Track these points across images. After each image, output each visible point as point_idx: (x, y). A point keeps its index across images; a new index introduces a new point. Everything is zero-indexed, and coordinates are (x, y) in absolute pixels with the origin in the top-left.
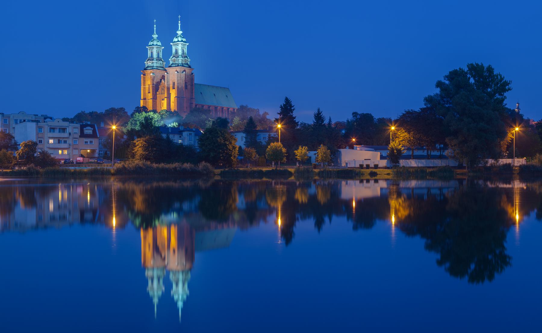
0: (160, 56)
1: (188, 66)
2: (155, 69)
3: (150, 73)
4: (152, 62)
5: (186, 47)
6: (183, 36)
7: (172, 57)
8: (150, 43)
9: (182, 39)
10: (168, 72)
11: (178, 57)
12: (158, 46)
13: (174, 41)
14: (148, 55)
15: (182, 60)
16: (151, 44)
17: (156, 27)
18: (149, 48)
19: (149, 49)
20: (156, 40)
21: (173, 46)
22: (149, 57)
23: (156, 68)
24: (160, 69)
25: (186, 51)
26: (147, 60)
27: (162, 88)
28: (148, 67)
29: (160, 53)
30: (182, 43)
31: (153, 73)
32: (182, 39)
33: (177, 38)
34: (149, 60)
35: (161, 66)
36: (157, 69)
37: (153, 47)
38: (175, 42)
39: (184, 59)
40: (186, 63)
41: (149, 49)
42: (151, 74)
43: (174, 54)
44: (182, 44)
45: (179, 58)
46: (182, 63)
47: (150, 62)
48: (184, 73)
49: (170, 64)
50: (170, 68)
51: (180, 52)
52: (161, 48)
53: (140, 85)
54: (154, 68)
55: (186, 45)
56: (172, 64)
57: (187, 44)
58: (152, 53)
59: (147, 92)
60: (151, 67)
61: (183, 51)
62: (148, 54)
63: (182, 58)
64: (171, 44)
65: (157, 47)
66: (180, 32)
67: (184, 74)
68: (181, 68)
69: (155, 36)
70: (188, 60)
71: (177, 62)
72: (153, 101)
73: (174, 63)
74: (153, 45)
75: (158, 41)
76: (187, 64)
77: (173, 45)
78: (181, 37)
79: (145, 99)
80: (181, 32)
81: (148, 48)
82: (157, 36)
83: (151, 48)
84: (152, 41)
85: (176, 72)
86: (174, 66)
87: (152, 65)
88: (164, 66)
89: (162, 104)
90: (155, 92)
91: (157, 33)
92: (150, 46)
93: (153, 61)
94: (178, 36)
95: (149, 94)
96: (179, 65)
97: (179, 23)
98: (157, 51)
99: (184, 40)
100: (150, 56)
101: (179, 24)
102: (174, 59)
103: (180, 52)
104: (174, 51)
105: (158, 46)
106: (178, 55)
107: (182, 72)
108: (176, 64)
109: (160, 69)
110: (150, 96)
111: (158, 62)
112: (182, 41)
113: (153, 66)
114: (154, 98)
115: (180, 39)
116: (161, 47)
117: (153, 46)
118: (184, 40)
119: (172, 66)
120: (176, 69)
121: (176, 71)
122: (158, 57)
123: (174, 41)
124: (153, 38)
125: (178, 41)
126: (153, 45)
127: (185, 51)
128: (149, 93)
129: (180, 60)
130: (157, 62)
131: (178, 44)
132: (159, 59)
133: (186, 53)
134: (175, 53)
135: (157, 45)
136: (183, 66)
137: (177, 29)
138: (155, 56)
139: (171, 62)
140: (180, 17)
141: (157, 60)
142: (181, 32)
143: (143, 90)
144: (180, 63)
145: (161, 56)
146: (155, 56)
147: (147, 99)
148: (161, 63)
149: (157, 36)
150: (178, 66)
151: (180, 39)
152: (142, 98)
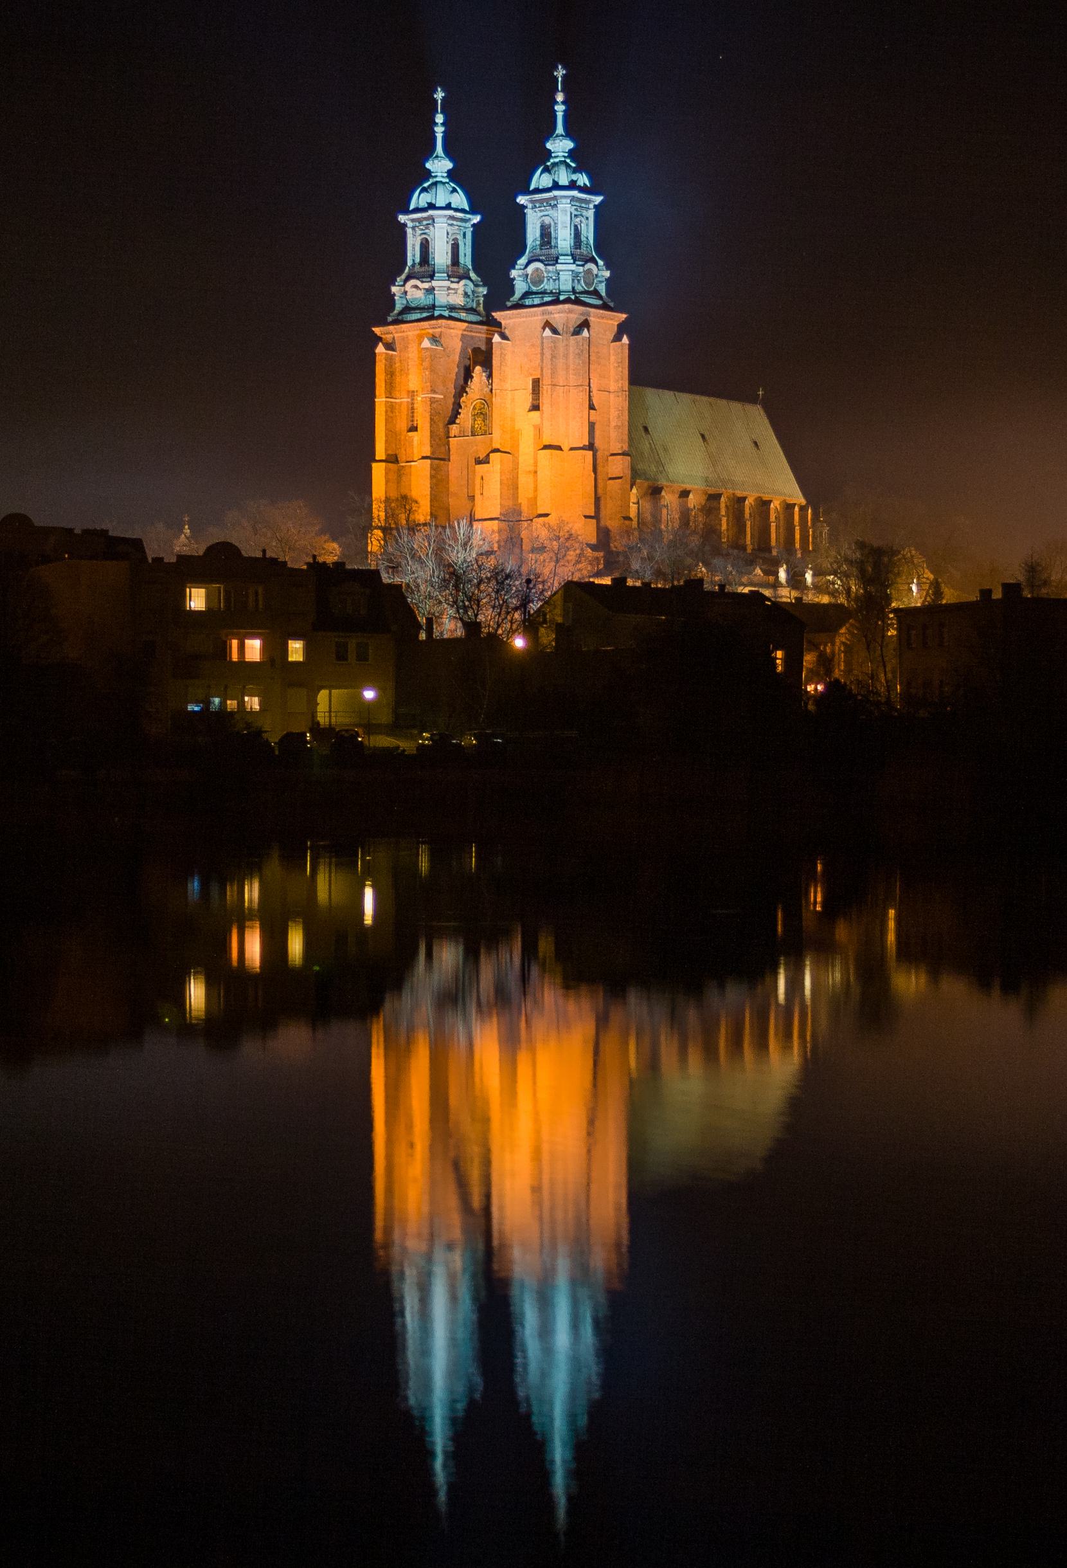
0: (462, 260)
1: (599, 302)
2: (441, 317)
3: (420, 338)
4: (426, 285)
5: (591, 214)
6: (580, 159)
7: (522, 261)
8: (419, 199)
9: (574, 177)
10: (507, 332)
11: (556, 261)
12: (456, 210)
13: (532, 187)
14: (409, 254)
15: (575, 275)
16: (423, 204)
17: (443, 124)
18: (413, 220)
19: (413, 228)
20: (444, 183)
21: (528, 211)
22: (409, 263)
23: (446, 314)
24: (463, 315)
25: (588, 233)
26: (403, 276)
27: (474, 408)
28: (407, 309)
29: (461, 244)
30: (575, 193)
31: (435, 339)
32: (574, 177)
33: (547, 170)
34: (418, 279)
35: (469, 306)
36: (451, 318)
37: (432, 218)
38: (537, 191)
39: (581, 269)
40: (592, 289)
41: (413, 228)
42: (426, 343)
43: (534, 248)
44: (573, 199)
45: (559, 267)
46: (573, 288)
47: (416, 287)
48: (585, 333)
49: (518, 295)
50: (514, 312)
51: (564, 240)
52: (466, 221)
53: (373, 395)
54: (437, 313)
55: (588, 202)
56: (527, 294)
57: (593, 197)
58: (425, 246)
59: (402, 424)
60: (422, 309)
61: (577, 234)
62: (409, 248)
63: (573, 267)
64: (521, 200)
65: (452, 218)
66: (560, 146)
67: (583, 339)
68: (570, 311)
69: (440, 166)
70: (600, 273)
71: (547, 286)
72: (431, 465)
73: (534, 289)
74: (432, 206)
75: (454, 190)
76: (596, 293)
77: (530, 206)
78: (568, 166)
79: (392, 459)
80: (569, 145)
81: (405, 225)
82: (450, 165)
83: (419, 220)
84: (425, 190)
85: (548, 332)
86: (537, 301)
87: (428, 301)
88: (478, 304)
89: (478, 480)
90: (441, 425)
91: (449, 152)
92: (417, 210)
93: (434, 283)
94: (555, 164)
95: (410, 434)
96: (562, 298)
97: (556, 102)
98: (448, 234)
99: (583, 180)
100: (418, 260)
101: (560, 109)
102: (537, 269)
103: (564, 240)
104: (533, 234)
105: (456, 210)
106: (553, 251)
107: (572, 329)
108: (544, 293)
109: (463, 315)
110: (420, 443)
111: (454, 286)
112: (573, 185)
113: (433, 307)
114: (439, 457)
115: (563, 178)
116: (468, 216)
117: (431, 212)
118: (580, 183)
119: (528, 302)
120: (546, 317)
121: (547, 324)
122: (455, 261)
123: (532, 187)
124: (428, 174)
125: (556, 186)
126: (432, 206)
127: (584, 232)
128: (414, 429)
129: (566, 275)
130: (449, 288)
131: (555, 198)
132: (456, 272)
133: (592, 242)
134: (538, 243)
135: (448, 207)
136: (577, 302)
137: (550, 132)
138: (441, 256)
139: (520, 287)
140: (560, 72)
141: (449, 276)
142: (569, 145)
143: (383, 418)
144: (563, 288)
145: (466, 258)
146: (441, 256)
147: (402, 457)
148: (470, 293)
149: (450, 165)
150: (556, 302)
151: (563, 178)
152: (380, 452)
